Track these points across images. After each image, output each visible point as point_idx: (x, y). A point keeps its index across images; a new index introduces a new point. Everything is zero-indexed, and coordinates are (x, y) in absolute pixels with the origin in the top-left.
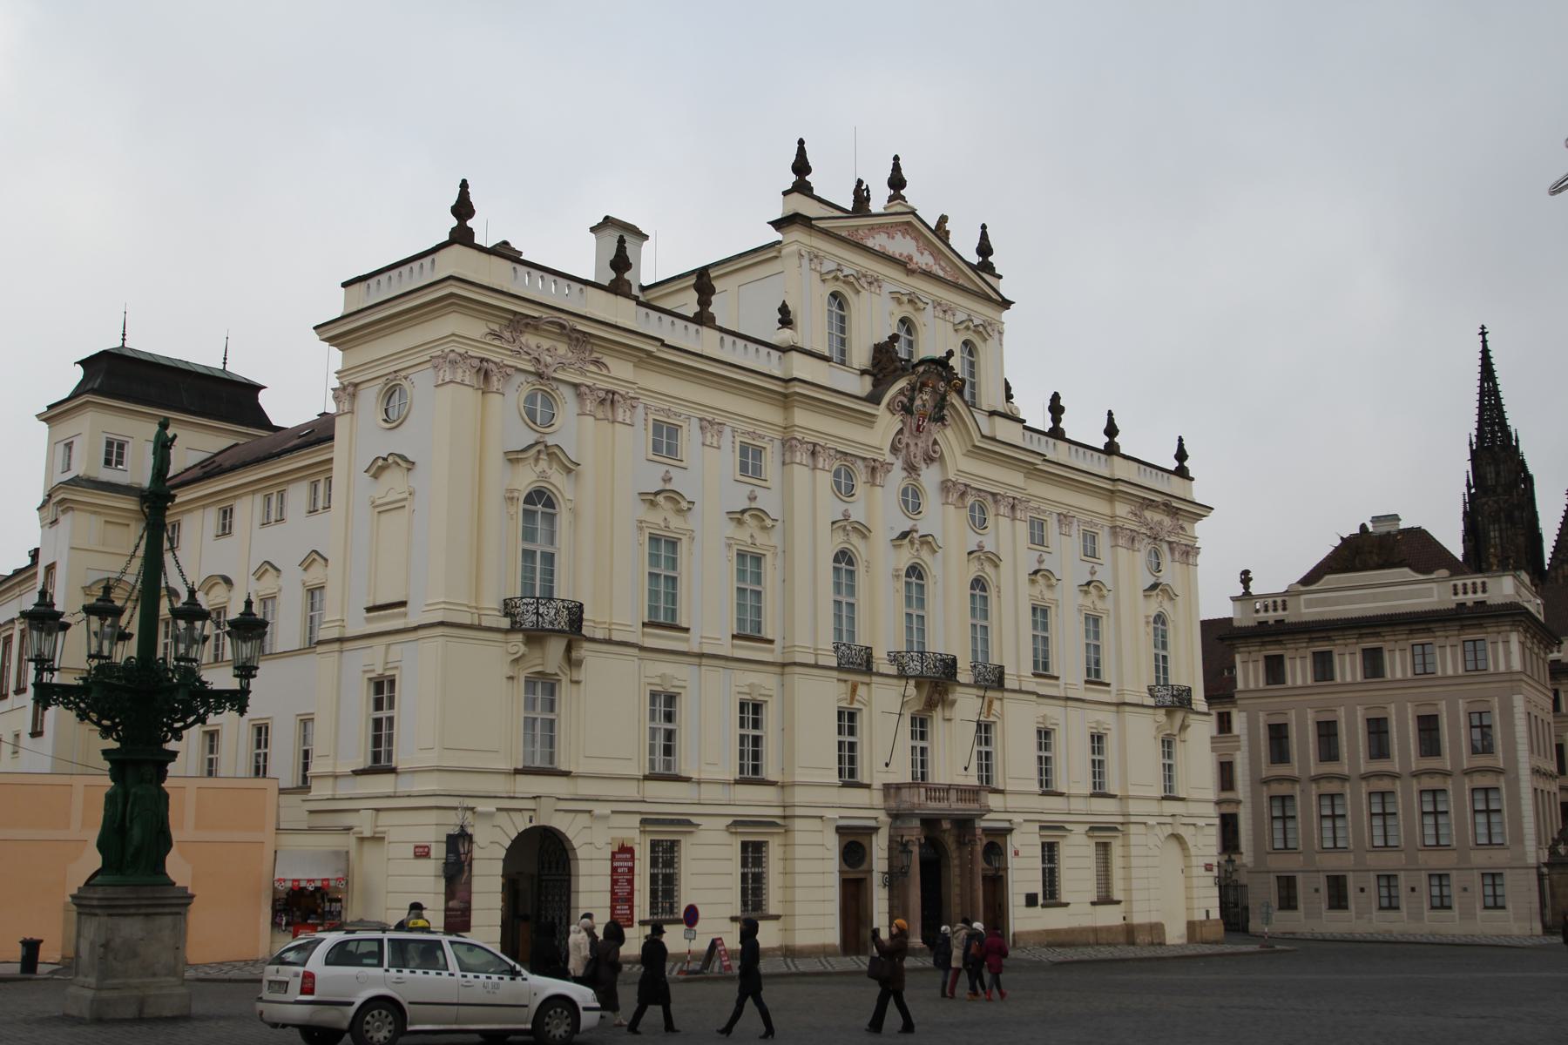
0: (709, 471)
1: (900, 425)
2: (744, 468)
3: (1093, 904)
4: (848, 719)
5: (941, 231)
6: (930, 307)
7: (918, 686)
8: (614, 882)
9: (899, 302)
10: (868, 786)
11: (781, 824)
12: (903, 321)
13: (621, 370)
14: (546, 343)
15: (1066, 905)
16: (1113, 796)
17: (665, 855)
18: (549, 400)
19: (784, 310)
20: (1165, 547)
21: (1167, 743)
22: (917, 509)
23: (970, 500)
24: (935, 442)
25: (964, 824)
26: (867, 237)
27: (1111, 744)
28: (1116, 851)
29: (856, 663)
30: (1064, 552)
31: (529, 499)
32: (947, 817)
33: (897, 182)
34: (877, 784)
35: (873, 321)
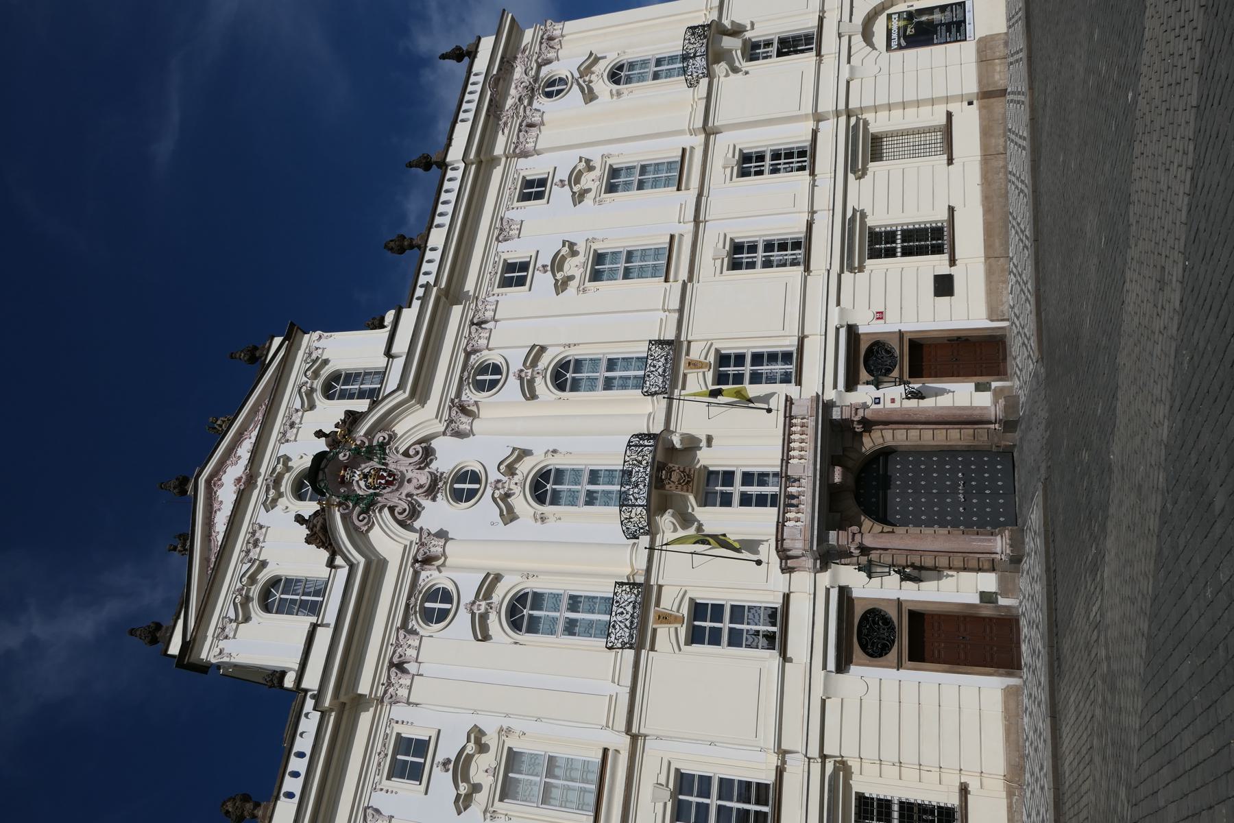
1: (386, 510)
2: (415, 773)
3: (950, 161)
4: (706, 624)
7: (662, 510)
9: (275, 501)
10: (787, 598)
15: (951, 210)
16: (815, 133)
20: (545, 71)
21: (753, 51)
22: (475, 477)
23: (470, 396)
24: (406, 454)
25: (839, 435)
27: (754, 140)
28: (878, 123)
29: (634, 617)
30: (539, 230)
32: (826, 474)
34: (779, 582)
35: (285, 547)
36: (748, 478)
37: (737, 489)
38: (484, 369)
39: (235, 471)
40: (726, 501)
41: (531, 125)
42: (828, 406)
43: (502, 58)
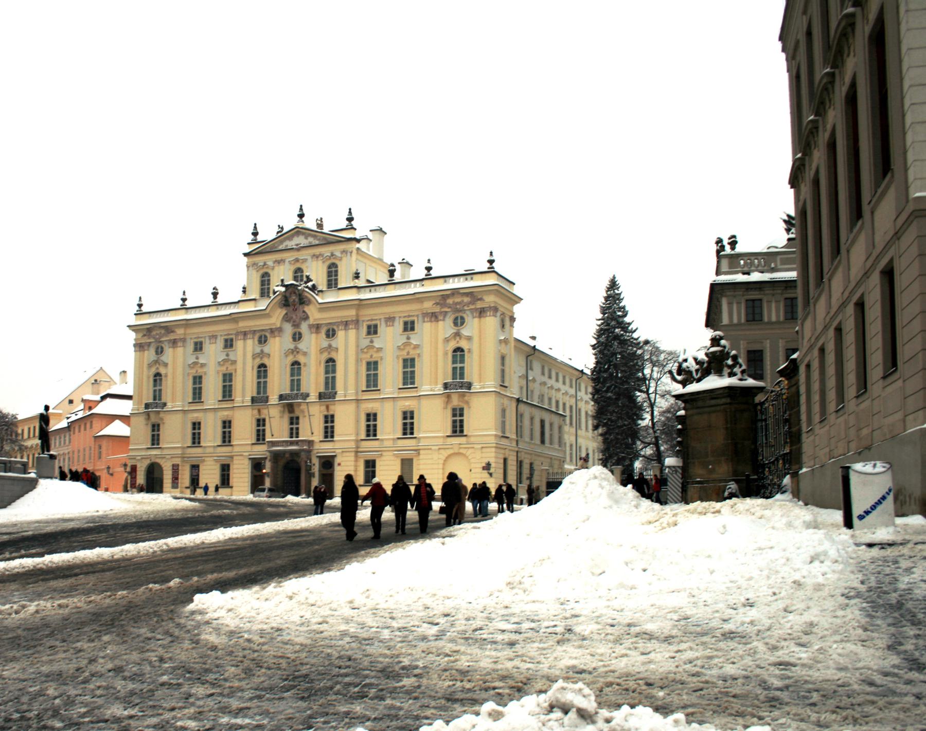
0: (213, 353)
4: (261, 422)
5: (320, 226)
6: (309, 258)
11: (232, 457)
13: (180, 332)
17: (195, 468)
18: (162, 348)
24: (304, 312)
31: (155, 376)
33: (301, 216)
36: (297, 429)
37: (294, 426)
38: (334, 330)
41: (436, 317)
42: (309, 452)
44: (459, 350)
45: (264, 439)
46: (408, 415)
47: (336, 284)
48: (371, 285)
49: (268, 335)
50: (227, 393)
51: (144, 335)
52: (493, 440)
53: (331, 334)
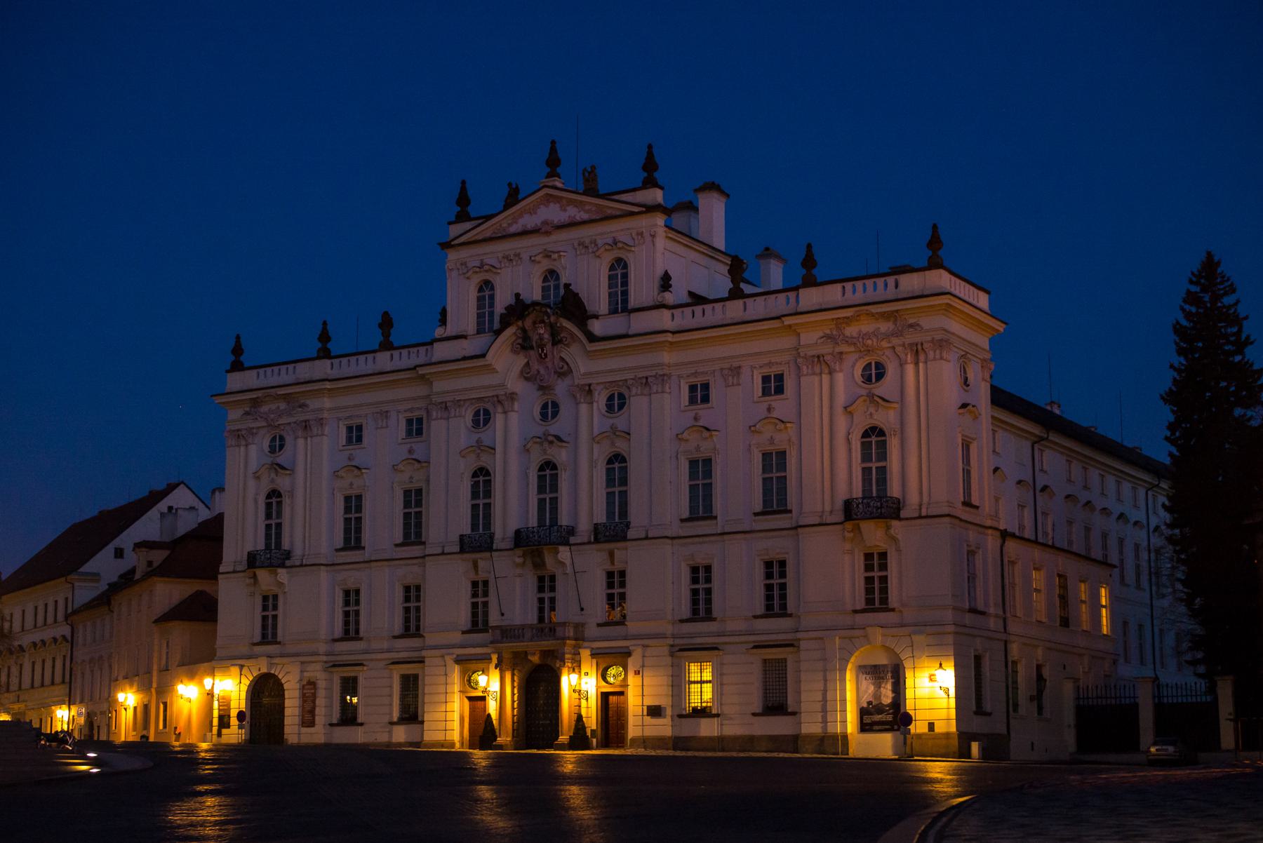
0: (384, 443)
3: (754, 714)
8: (304, 701)
12: (551, 274)
14: (273, 407)
18: (282, 438)
19: (444, 312)
24: (562, 359)
26: (510, 225)
37: (547, 595)
39: (553, 213)
40: (541, 589)
43: (897, 311)
44: (874, 433)
45: (486, 622)
46: (776, 569)
47: (625, 301)
48: (697, 299)
49: (489, 407)
50: (413, 531)
51: (247, 413)
52: (949, 615)
53: (616, 403)
